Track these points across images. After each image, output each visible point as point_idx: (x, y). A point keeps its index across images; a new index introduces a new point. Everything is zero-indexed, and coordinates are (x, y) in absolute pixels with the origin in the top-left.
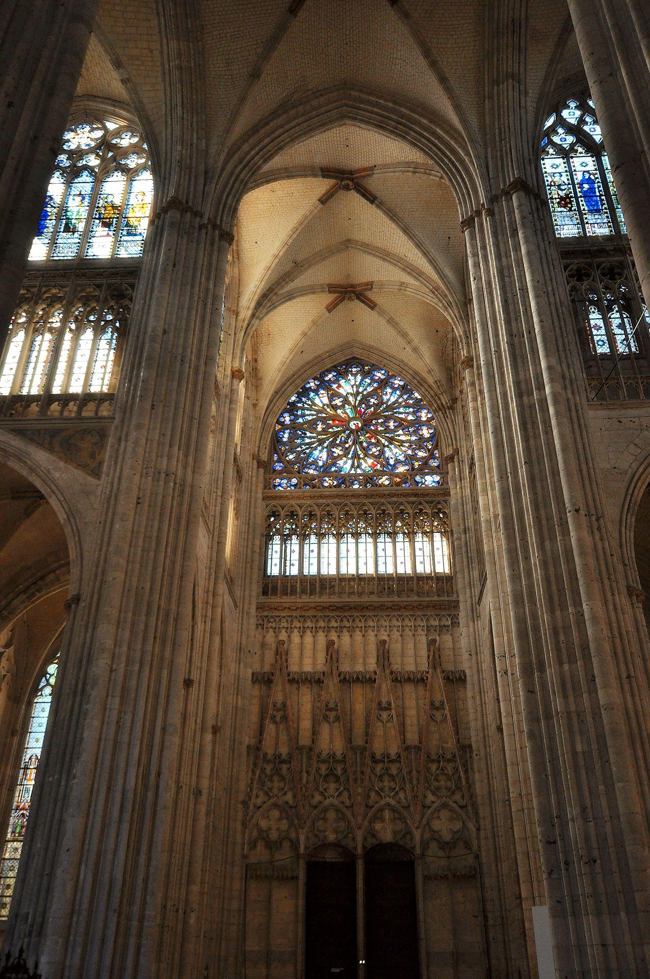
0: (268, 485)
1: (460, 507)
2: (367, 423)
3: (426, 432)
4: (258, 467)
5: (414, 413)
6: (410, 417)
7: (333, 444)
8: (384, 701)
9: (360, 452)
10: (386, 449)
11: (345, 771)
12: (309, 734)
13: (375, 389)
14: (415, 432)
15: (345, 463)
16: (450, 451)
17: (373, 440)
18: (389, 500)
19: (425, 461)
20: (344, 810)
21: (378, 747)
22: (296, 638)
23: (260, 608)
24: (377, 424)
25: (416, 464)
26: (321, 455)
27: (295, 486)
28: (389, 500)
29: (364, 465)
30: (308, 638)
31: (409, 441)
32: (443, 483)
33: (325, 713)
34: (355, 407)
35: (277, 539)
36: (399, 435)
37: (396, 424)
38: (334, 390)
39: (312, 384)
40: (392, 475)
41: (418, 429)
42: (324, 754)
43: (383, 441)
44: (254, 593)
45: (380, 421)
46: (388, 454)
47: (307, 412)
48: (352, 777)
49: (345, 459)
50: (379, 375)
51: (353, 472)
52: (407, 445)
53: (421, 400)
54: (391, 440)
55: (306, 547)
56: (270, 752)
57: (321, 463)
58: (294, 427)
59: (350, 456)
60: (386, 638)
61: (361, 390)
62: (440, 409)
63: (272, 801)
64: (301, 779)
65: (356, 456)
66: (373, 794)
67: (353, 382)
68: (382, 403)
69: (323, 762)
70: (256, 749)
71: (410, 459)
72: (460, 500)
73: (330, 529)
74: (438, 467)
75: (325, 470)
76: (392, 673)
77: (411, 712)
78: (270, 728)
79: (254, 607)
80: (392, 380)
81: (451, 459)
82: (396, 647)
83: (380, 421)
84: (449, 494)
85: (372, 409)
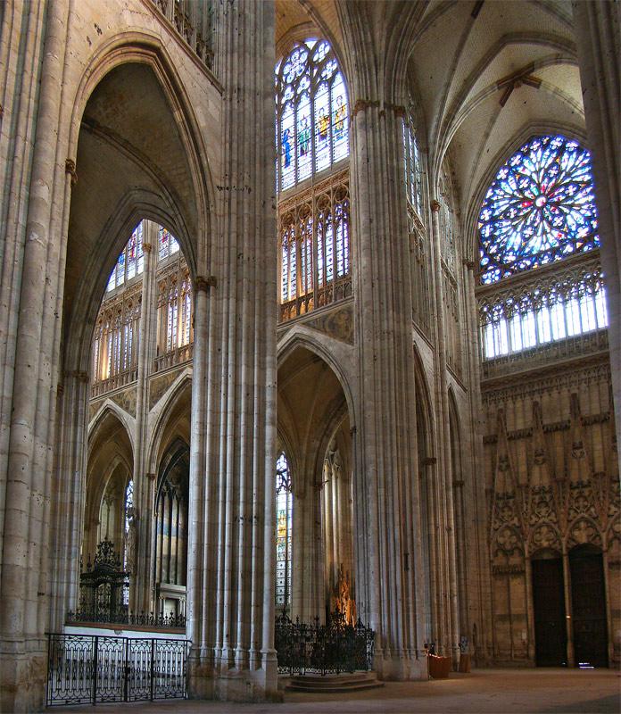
0: (480, 281)
2: (550, 195)
4: (468, 270)
7: (525, 227)
8: (577, 442)
11: (552, 498)
12: (525, 475)
13: (555, 158)
20: (553, 525)
21: (574, 477)
22: (511, 406)
23: (483, 386)
24: (558, 195)
27: (499, 275)
30: (519, 405)
31: (588, 203)
33: (537, 458)
34: (538, 186)
35: (490, 327)
36: (578, 199)
40: (573, 241)
42: (537, 489)
43: (566, 210)
44: (478, 376)
46: (570, 221)
47: (501, 203)
48: (557, 502)
50: (556, 143)
51: (543, 249)
54: (570, 207)
56: (501, 492)
58: (493, 220)
60: (576, 391)
63: (505, 524)
64: (522, 508)
65: (544, 232)
66: (572, 512)
68: (560, 172)
69: (536, 494)
70: (490, 492)
76: (582, 419)
77: (598, 447)
78: (499, 475)
79: (479, 387)
82: (583, 398)
85: (554, 180)
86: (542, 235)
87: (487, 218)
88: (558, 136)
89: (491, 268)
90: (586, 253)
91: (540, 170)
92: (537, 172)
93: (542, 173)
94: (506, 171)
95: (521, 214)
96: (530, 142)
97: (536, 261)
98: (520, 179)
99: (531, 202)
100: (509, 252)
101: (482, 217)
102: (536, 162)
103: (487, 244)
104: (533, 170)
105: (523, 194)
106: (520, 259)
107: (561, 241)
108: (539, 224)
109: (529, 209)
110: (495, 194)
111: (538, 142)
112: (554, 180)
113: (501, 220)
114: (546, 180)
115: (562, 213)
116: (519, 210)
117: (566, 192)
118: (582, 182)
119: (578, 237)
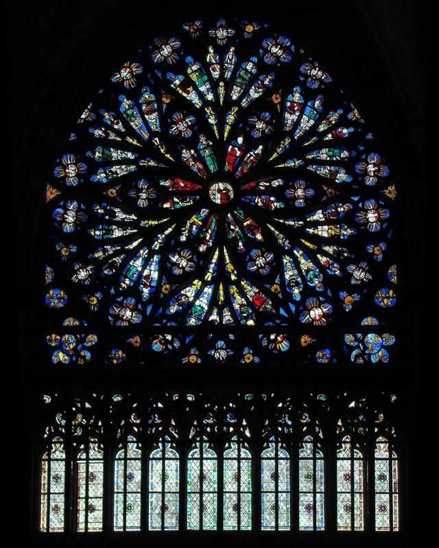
2: (243, 185)
5: (348, 165)
6: (342, 177)
7: (172, 245)
9: (230, 267)
10: (286, 260)
15: (198, 294)
17: (259, 237)
19: (367, 291)
24: (270, 191)
25: (348, 300)
29: (238, 301)
36: (316, 224)
37: (311, 192)
38: (173, 93)
39: (125, 73)
41: (356, 209)
43: (281, 239)
45: (276, 183)
47: (116, 155)
49: (198, 283)
51: (214, 317)
52: (330, 249)
54: (296, 236)
55: (118, 468)
58: (87, 193)
59: (209, 277)
71: (335, 285)
73: (166, 425)
86: (215, 282)
87: (72, 180)
89: (69, 322)
93: (231, 118)
94: (137, 70)
95: (167, 205)
97: (191, 345)
98: (172, 108)
104: (210, 97)
106: (147, 329)
108: (210, 252)
116: (165, 194)
117: (289, 192)
118: (330, 182)
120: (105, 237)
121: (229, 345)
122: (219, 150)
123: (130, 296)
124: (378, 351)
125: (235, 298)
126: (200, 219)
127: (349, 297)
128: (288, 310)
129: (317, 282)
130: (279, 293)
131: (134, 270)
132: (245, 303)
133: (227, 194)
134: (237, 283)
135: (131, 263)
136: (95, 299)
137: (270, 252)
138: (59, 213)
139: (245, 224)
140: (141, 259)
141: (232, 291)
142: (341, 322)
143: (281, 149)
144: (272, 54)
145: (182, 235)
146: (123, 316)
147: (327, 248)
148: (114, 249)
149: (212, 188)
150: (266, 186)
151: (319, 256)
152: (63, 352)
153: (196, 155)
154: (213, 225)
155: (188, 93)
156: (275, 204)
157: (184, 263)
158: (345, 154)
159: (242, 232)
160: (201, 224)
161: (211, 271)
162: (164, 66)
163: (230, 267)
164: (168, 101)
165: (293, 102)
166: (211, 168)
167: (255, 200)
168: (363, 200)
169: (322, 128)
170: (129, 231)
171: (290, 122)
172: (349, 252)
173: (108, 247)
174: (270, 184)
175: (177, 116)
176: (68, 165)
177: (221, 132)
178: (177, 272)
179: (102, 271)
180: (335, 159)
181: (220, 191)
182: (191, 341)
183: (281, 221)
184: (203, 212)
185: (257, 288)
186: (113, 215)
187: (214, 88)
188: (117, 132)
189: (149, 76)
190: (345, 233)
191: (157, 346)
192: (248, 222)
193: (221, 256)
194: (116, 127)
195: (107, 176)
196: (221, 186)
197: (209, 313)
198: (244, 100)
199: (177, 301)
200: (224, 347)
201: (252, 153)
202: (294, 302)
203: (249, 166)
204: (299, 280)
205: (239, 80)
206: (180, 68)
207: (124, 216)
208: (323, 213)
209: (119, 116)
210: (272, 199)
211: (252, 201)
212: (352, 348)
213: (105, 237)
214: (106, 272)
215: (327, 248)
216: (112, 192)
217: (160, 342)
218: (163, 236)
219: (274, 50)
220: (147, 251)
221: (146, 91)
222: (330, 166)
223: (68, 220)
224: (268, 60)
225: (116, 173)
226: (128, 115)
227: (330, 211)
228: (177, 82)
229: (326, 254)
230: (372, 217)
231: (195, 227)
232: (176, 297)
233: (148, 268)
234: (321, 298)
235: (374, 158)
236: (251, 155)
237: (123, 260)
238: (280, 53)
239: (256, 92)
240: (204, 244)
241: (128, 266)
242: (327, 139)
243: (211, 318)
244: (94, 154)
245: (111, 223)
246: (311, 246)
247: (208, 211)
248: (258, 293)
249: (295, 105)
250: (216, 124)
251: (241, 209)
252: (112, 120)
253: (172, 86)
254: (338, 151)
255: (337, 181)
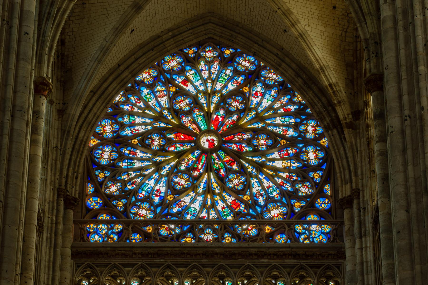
0: (82, 235)
1: (359, 278)
2: (225, 137)
3: (312, 156)
4: (65, 208)
5: (296, 127)
6: (291, 133)
7: (175, 171)
9: (215, 185)
10: (254, 181)
13: (241, 86)
14: (297, 157)
15: (193, 201)
16: (345, 191)
17: (235, 167)
18: (257, 262)
24: (241, 141)
25: (297, 205)
26: (156, 186)
27: (119, 234)
28: (257, 262)
29: (221, 204)
31: (287, 169)
32: (336, 235)
37: (270, 142)
38: (177, 86)
39: (145, 75)
41: (301, 152)
43: (250, 168)
45: (246, 137)
46: (256, 189)
47: (138, 120)
49: (192, 194)
50: (245, 63)
51: (204, 214)
52: (284, 175)
53: (305, 107)
57: (156, 200)
58: (118, 142)
59: (200, 190)
61: (218, 87)
62: (335, 127)
65: (209, 190)
67: (206, 76)
68: (247, 109)
72: (358, 268)
74: (329, 211)
75: (164, 211)
80: (264, 73)
81: (347, 203)
83: (246, 137)
84: (343, 256)
85: (235, 118)
88: (254, 55)
90: (281, 247)
91: (214, 92)
92: (209, 95)
94: (154, 73)
95: (172, 149)
96: (201, 45)
97: (189, 231)
98: (176, 94)
99: (193, 138)
100: (143, 200)
101: (99, 130)
102: (207, 78)
103: (101, 175)
104: (202, 88)
105: (180, 119)
106: (156, 223)
107: (237, 215)
108: (201, 175)
109: (187, 147)
110: (127, 102)
111: (214, 49)
112: (235, 118)
113: (134, 147)
114: (222, 112)
115: (242, 171)
116: (170, 142)
117: (255, 142)
118: (283, 137)
119: (267, 216)
120: (129, 167)
121: (215, 231)
122: (208, 116)
123: (145, 202)
124: (319, 236)
125: (218, 203)
126: (194, 156)
127: (298, 203)
128: (255, 210)
129: (275, 194)
130: (249, 200)
131: (149, 186)
132: (225, 206)
133: (213, 142)
134: (220, 194)
135: (147, 182)
136: (121, 203)
137: (243, 176)
138: (98, 153)
139: (225, 160)
140: (153, 180)
141: (216, 199)
142: (292, 218)
143: (249, 117)
144: (243, 66)
145: (182, 166)
146: (140, 214)
147: (281, 174)
148: (135, 174)
149: (203, 139)
150: (240, 139)
151: (276, 179)
152: (98, 235)
153: (192, 120)
154: (203, 160)
155: (187, 86)
156: (246, 148)
157: (183, 182)
158: (293, 120)
159: (223, 164)
160: (195, 159)
161: (202, 187)
162: (171, 71)
163: (215, 185)
164: (174, 90)
165: (257, 92)
166: (202, 127)
167: (232, 146)
168: (305, 146)
169: (276, 106)
170: (146, 163)
171: (255, 102)
172: (298, 176)
173: (131, 173)
174: (242, 137)
175: (179, 99)
176: (106, 126)
177: (209, 107)
178: (178, 187)
179: (127, 186)
180: (285, 123)
181: (208, 140)
182: (187, 230)
183: (250, 158)
184: (197, 153)
185: (234, 197)
186: (135, 154)
187: (205, 81)
188: (140, 108)
189: (161, 77)
190: (294, 165)
191: (164, 232)
192: (228, 159)
193: (209, 179)
194: (138, 104)
195: (132, 132)
196: (209, 138)
197: (201, 211)
198: (224, 90)
199: (178, 205)
200: (211, 233)
201: (230, 119)
202: (260, 206)
203: (228, 127)
204: (263, 192)
205: (220, 79)
206: (182, 72)
207: (142, 155)
208: (278, 153)
209: (140, 99)
210: (244, 145)
211: (230, 147)
212: (300, 234)
213: (129, 167)
214: (129, 187)
215: (281, 174)
216: (135, 141)
217: (166, 229)
218: (169, 166)
219: (244, 63)
220: (158, 175)
221: (159, 85)
222: (283, 127)
223: (104, 157)
224: (240, 68)
225: (138, 130)
226: (147, 98)
227: (283, 153)
228: (180, 80)
229: (281, 177)
230: (312, 156)
231: (190, 161)
232: (177, 202)
233: (158, 185)
234: (278, 204)
235: (312, 123)
236: (229, 121)
237: (141, 180)
238: (248, 65)
239: (232, 85)
240: (197, 171)
241: (145, 184)
242: (280, 112)
243: (202, 215)
244: (123, 119)
245: (132, 159)
246: (271, 173)
247: (200, 152)
248: (235, 200)
249: (258, 93)
250: (205, 103)
251: (223, 151)
252: (136, 100)
253: (176, 82)
254: (288, 119)
255: (287, 135)
